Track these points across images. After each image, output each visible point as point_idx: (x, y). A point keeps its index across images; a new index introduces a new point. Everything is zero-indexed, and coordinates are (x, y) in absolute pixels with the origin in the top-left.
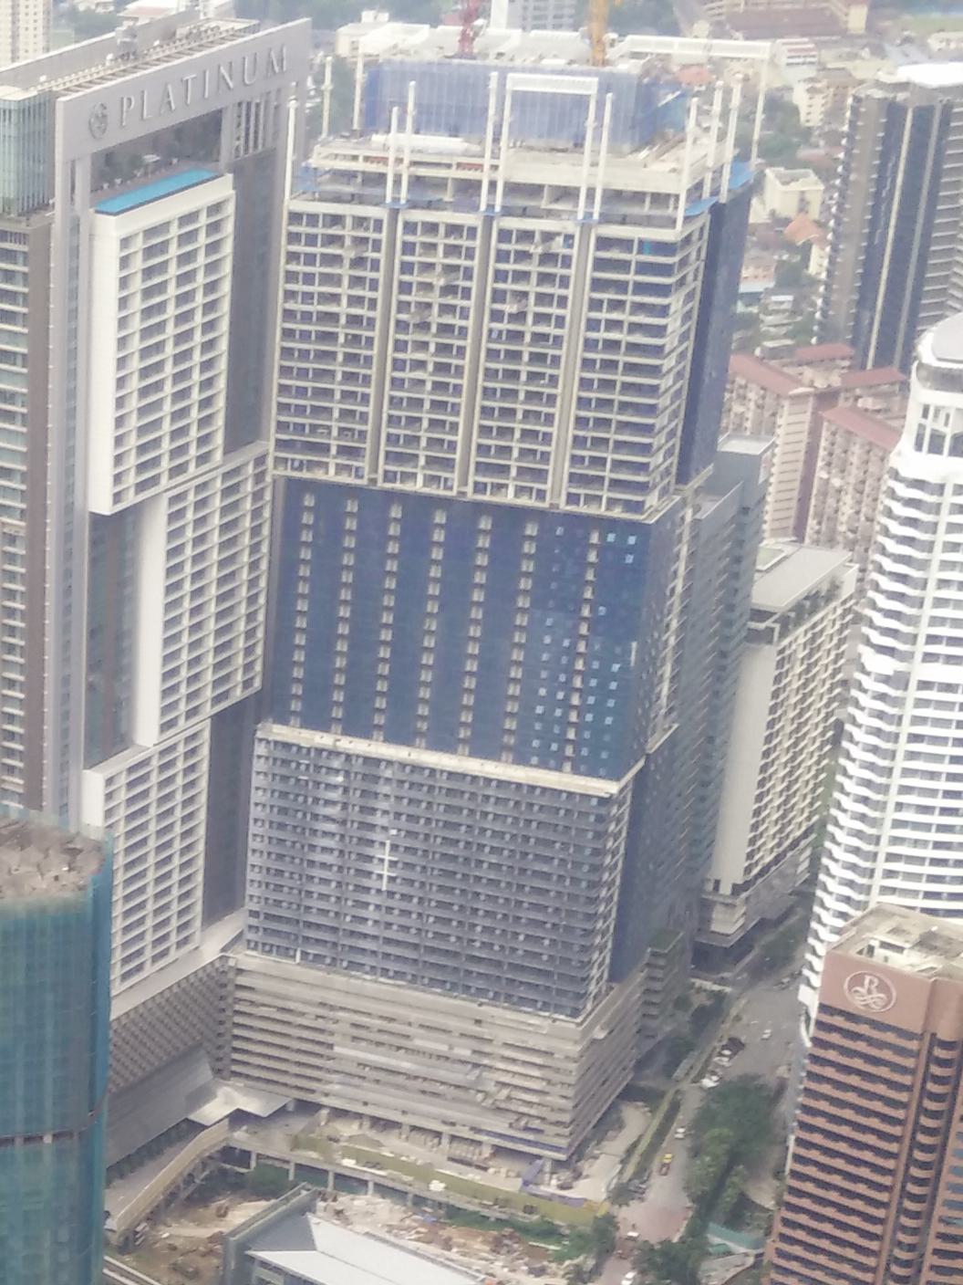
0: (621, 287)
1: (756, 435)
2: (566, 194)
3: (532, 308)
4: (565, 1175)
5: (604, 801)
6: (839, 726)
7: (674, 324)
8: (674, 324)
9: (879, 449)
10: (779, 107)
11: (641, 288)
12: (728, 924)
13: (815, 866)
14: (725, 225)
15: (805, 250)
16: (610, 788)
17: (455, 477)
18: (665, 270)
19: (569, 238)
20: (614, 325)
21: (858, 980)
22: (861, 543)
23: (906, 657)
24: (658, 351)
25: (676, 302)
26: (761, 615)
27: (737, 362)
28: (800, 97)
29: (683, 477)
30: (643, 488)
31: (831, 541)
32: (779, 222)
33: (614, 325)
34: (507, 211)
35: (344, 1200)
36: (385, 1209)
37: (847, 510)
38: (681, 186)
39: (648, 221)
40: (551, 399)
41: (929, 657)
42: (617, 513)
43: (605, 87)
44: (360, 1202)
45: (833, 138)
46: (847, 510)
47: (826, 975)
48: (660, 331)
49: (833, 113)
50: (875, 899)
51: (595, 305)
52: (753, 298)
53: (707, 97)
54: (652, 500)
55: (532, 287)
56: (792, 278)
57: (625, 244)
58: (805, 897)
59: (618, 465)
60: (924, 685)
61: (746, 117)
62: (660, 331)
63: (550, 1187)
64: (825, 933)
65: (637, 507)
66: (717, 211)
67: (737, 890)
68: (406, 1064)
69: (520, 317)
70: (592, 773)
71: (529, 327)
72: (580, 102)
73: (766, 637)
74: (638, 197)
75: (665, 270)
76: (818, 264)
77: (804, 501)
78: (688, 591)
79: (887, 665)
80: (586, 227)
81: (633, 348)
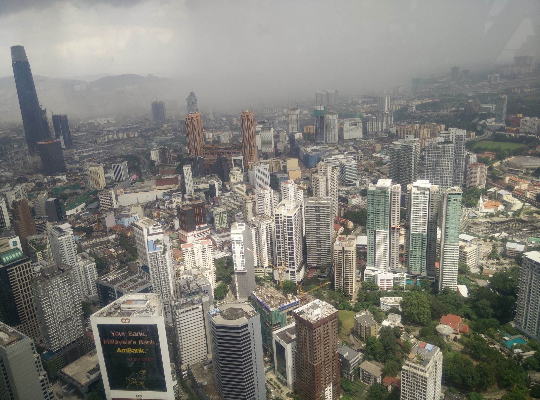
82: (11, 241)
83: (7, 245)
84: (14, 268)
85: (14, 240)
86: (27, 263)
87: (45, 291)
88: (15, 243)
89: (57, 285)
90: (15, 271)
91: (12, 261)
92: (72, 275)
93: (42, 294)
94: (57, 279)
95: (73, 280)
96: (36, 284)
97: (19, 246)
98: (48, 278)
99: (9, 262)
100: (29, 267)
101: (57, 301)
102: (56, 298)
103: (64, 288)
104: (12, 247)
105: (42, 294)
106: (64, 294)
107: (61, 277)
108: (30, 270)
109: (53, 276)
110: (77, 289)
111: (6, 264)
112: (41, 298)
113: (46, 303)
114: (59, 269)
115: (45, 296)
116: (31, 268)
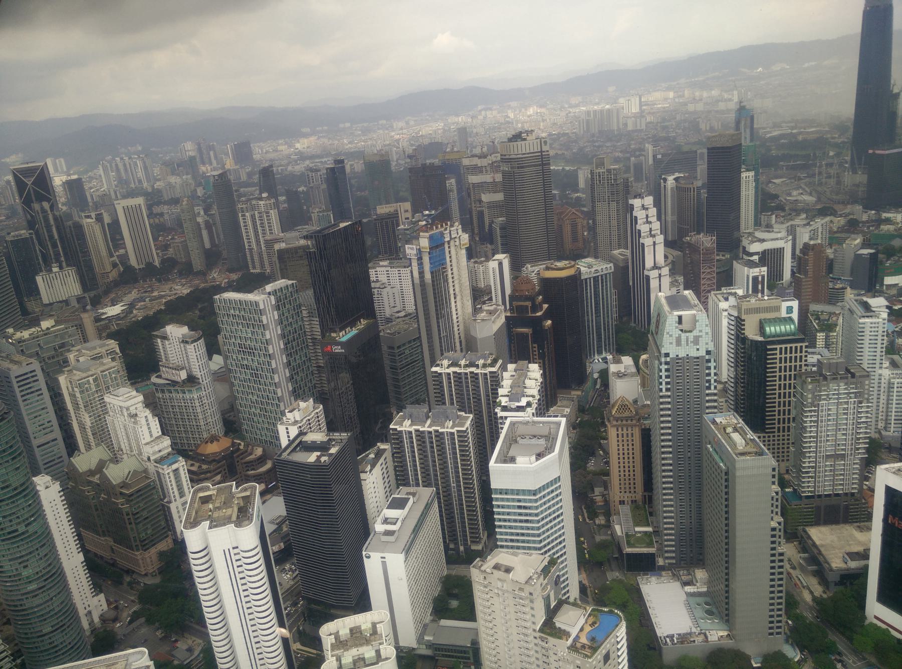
82: (785, 305)
83: (778, 309)
84: (778, 347)
85: (789, 304)
86: (799, 345)
87: (814, 397)
88: (790, 310)
89: (837, 394)
90: (778, 352)
91: (778, 336)
92: (867, 387)
93: (810, 401)
94: (839, 386)
95: (866, 396)
96: (804, 382)
97: (795, 316)
98: (825, 378)
99: (774, 336)
100: (801, 352)
101: (829, 420)
102: (829, 415)
103: (847, 403)
104: (784, 314)
105: (810, 401)
106: (844, 414)
107: (846, 384)
108: (801, 357)
109: (834, 379)
110: (867, 412)
111: (769, 337)
112: (805, 406)
113: (811, 416)
114: (848, 371)
115: (813, 405)
116: (804, 354)
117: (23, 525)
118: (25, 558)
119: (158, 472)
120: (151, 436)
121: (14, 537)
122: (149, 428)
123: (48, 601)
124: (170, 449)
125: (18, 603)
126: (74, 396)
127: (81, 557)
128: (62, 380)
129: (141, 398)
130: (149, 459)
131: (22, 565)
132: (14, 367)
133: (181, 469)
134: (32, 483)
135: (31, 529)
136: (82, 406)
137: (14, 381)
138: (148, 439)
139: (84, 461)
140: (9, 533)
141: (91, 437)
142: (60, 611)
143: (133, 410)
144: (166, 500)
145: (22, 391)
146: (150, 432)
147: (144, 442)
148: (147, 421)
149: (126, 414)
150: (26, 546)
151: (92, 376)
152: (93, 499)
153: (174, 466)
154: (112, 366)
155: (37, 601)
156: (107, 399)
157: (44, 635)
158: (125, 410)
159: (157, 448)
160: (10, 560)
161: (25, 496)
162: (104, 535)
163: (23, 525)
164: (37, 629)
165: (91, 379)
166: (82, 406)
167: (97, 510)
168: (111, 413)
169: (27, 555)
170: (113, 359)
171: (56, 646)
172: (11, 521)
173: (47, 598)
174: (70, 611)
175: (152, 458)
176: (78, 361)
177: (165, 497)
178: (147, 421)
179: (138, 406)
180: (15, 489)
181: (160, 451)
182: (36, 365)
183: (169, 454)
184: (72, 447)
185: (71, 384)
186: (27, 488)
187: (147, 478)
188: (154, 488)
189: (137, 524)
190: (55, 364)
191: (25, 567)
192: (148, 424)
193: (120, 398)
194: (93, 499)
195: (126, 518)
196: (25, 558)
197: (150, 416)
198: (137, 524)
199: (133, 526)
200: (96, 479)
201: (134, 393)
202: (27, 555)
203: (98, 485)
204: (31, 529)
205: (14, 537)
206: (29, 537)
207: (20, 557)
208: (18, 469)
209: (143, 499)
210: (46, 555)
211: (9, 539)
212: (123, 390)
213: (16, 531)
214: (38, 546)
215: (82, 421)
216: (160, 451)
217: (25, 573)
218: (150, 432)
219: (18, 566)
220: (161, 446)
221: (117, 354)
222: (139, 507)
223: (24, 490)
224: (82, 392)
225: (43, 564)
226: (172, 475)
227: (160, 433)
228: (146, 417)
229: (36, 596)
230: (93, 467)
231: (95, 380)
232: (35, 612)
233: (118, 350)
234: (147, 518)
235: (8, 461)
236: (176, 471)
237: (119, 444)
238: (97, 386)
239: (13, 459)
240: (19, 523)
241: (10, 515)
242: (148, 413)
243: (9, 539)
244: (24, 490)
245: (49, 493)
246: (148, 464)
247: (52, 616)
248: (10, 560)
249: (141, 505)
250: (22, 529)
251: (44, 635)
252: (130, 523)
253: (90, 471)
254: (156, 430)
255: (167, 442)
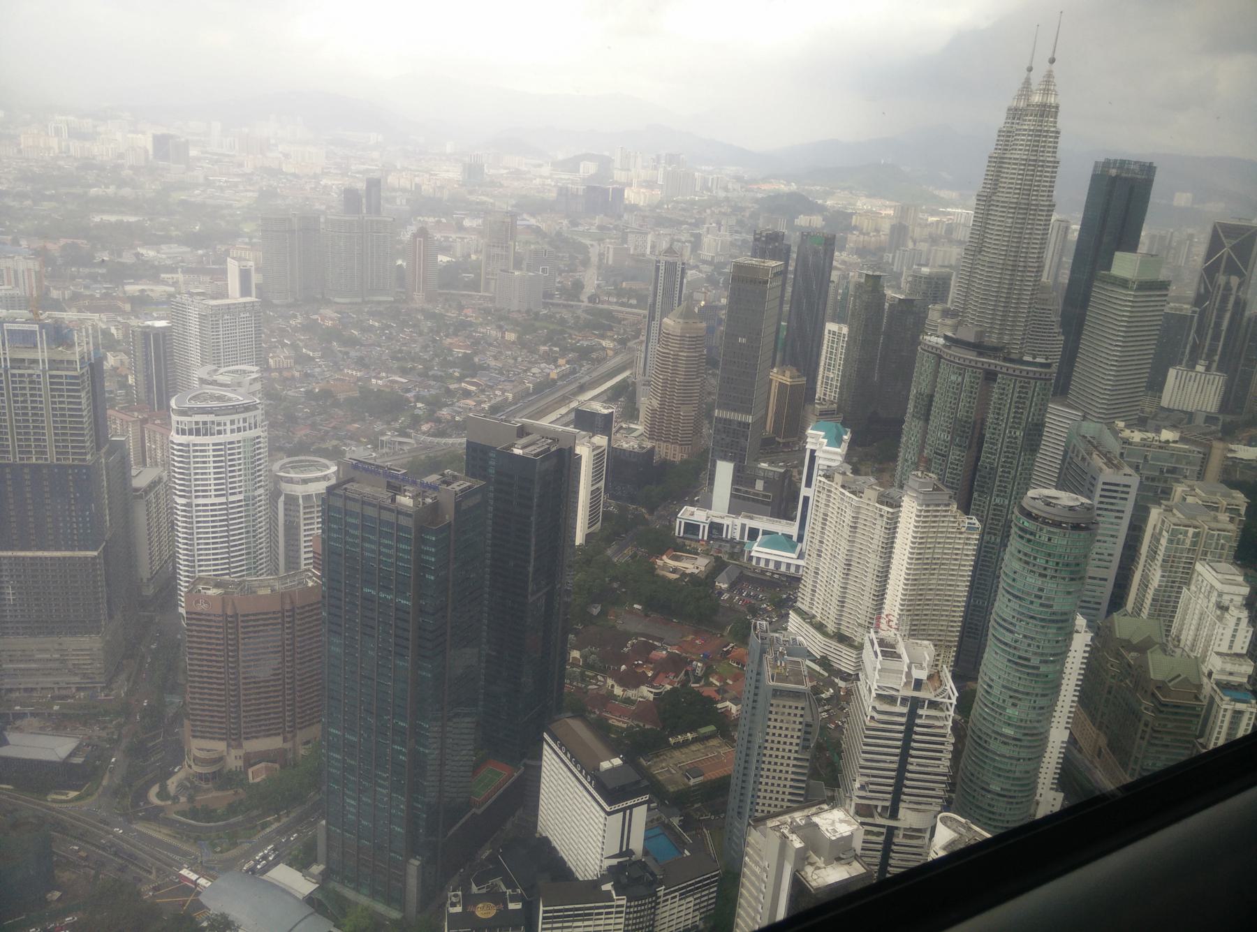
0: (61, 390)
1: (123, 435)
2: (35, 361)
3: (29, 399)
4: (106, 691)
5: (94, 558)
6: (172, 522)
7: (84, 401)
8: (84, 401)
9: (165, 436)
10: (106, 333)
11: (68, 390)
12: (149, 591)
13: (175, 568)
14: (95, 369)
15: (126, 377)
16: (95, 553)
17: (11, 456)
18: (78, 384)
19: (38, 376)
20: (61, 403)
21: (197, 602)
22: (167, 464)
23: (189, 497)
24: (80, 410)
25: (83, 394)
26: (136, 490)
27: (110, 412)
28: (113, 330)
29: (99, 448)
30: (85, 454)
31: (157, 465)
32: (115, 369)
33: (61, 403)
34: (12, 368)
35: (18, 723)
36: (35, 722)
37: (159, 455)
38: (77, 358)
39: (67, 370)
40: (43, 428)
41: (197, 497)
42: (76, 462)
43: (42, 326)
44: (25, 722)
45: (128, 343)
46: (159, 455)
47: (186, 602)
48: (80, 403)
49: (126, 336)
50: (197, 575)
51: (53, 396)
52: (111, 392)
53: (80, 330)
54: (88, 457)
55: (27, 392)
56: (123, 385)
57: (61, 377)
58: (174, 577)
59: (73, 447)
60: (197, 505)
61: (95, 337)
62: (80, 403)
63: (102, 696)
64: (183, 587)
65: (84, 460)
66: (91, 365)
67: (149, 580)
68: (34, 666)
69: (25, 401)
70: (87, 549)
71: (29, 405)
72: (33, 332)
73: (141, 497)
74: (62, 361)
75: (78, 384)
76: (131, 380)
77: (144, 452)
78: (108, 485)
79: (183, 501)
80: (44, 371)
81: (70, 409)
117: (1039, 659)
118: (1020, 696)
119: (1212, 700)
120: (1230, 647)
121: (1022, 665)
122: (1234, 636)
123: (1011, 758)
124: (1245, 680)
125: (984, 737)
126: (1158, 541)
127: (1065, 735)
128: (1155, 514)
129: (1246, 590)
130: (1210, 674)
131: (1012, 700)
132: (1107, 470)
133: (1246, 716)
134: (1074, 619)
135: (1043, 669)
136: (1160, 558)
137: (1100, 486)
138: (1224, 649)
139: (1123, 626)
140: (1020, 657)
141: (1148, 601)
142: (1018, 779)
143: (1226, 600)
144: (1201, 740)
145: (1101, 503)
146: (1232, 642)
147: (1217, 649)
148: (1237, 624)
149: (1213, 599)
150: (1027, 683)
151: (1196, 527)
152: (1113, 677)
153: (1240, 706)
154: (1227, 527)
155: (1004, 750)
156: (1199, 567)
157: (989, 792)
158: (1215, 593)
159: (1229, 667)
160: (1004, 687)
161: (1059, 628)
162: (1100, 728)
163: (1039, 659)
164: (985, 778)
165: (1191, 531)
166: (1160, 558)
167: (1109, 692)
168: (1193, 588)
169: (1023, 693)
170: (1232, 520)
171: (993, 813)
172: (1029, 645)
173: (1015, 755)
174: (1029, 785)
175: (1214, 676)
176: (1185, 499)
177: (1201, 736)
178: (1237, 624)
179: (1236, 598)
180: (1054, 613)
181: (1231, 674)
182: (1134, 481)
183: (1241, 685)
184: (1117, 601)
185: (1163, 522)
186: (1066, 621)
187: (1197, 698)
188: (1198, 716)
189: (1150, 744)
190: (1156, 490)
191: (1014, 705)
192: (1236, 630)
193: (1219, 576)
194: (1113, 677)
195: (1142, 727)
196: (1020, 696)
197: (1245, 621)
198: (1150, 744)
199: (1145, 743)
200: (1131, 656)
201: (1240, 579)
202: (1023, 693)
203: (1129, 665)
204: (1043, 669)
205: (1022, 665)
206: (1037, 675)
207: (1016, 691)
208: (1069, 593)
209: (1175, 720)
210: (1042, 708)
211: (1016, 664)
212: (1224, 566)
213: (1029, 660)
214: (1039, 691)
215: (1151, 575)
216: (1231, 674)
217: (1010, 711)
218: (1232, 642)
219: (1007, 699)
220: (1236, 668)
221: (1240, 515)
222: (1165, 726)
223: (1062, 621)
224: (1170, 541)
225: (1033, 715)
226: (1229, 714)
227: (1244, 651)
228: (1239, 619)
229: (1005, 743)
230: (1136, 640)
231: (1196, 535)
232: (994, 760)
233: (1243, 511)
234: (1167, 746)
235: (1064, 579)
236: (1241, 713)
237: (1180, 631)
238: (1194, 544)
239: (1072, 579)
240: (1035, 654)
241: (1032, 639)
242: (1244, 614)
243: (1016, 664)
244: (1062, 621)
245: (1081, 641)
246: (1205, 680)
247: (1008, 778)
248: (1004, 687)
249: (1170, 725)
250: (1035, 661)
251: (989, 792)
252: (1142, 738)
253: (1129, 641)
254: (1242, 645)
255: (1247, 668)
